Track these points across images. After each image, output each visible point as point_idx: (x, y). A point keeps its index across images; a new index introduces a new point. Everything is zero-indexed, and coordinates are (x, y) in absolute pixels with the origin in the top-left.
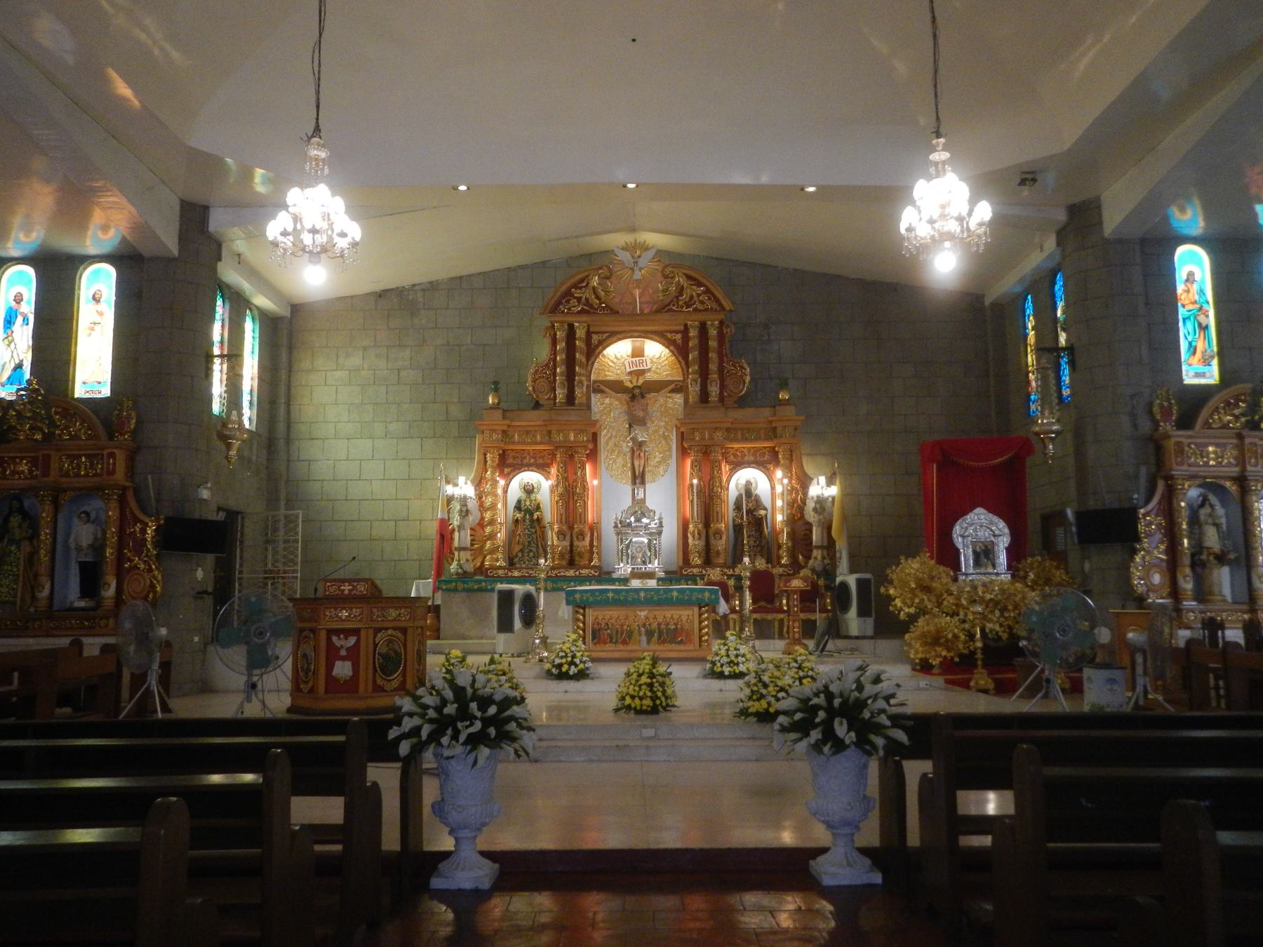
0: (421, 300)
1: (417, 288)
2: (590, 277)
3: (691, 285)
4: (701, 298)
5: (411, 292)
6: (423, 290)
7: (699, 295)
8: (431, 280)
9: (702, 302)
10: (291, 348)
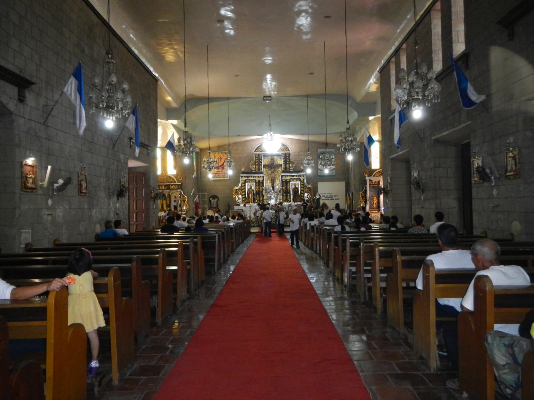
9: (285, 149)
10: (200, 158)
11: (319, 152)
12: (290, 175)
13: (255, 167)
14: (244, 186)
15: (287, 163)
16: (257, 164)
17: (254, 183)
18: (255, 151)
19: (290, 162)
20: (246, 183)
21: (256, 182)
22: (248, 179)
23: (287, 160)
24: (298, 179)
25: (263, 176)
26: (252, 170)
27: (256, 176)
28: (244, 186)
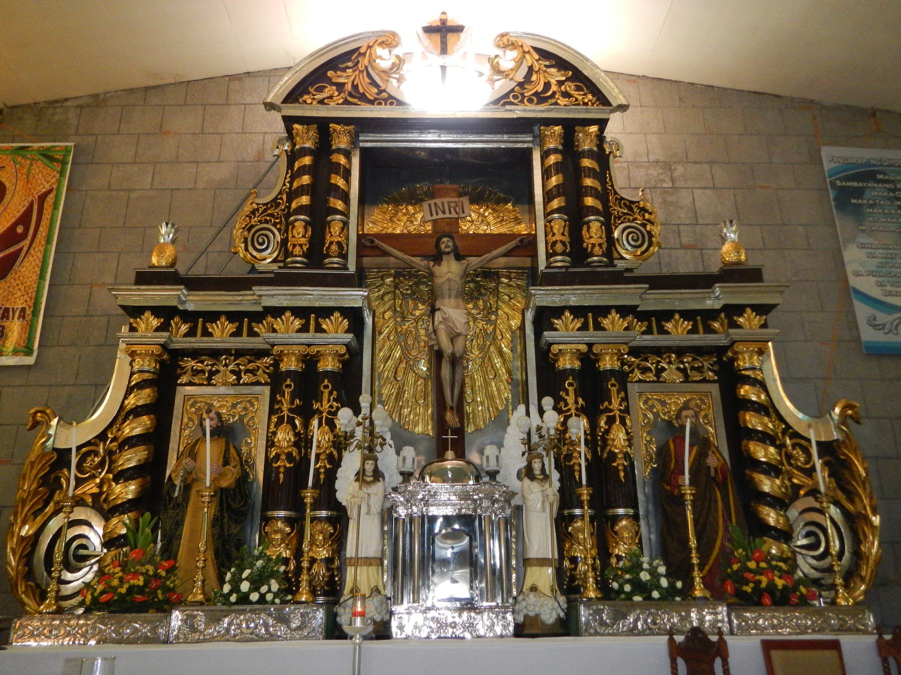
0: (73, 121)
1: (69, 104)
2: (362, 51)
3: (546, 66)
4: (563, 88)
5: (57, 110)
6: (81, 107)
7: (560, 83)
8: (95, 92)
9: (566, 95)
11: (827, 166)
12: (624, 311)
13: (284, 242)
14: (137, 412)
15: (593, 211)
16: (301, 210)
17: (267, 390)
18: (293, 96)
19: (616, 210)
20: (183, 392)
21: (276, 380)
22: (198, 342)
24: (698, 351)
25: (354, 317)
26: (253, 269)
27: (277, 312)
28: (137, 412)
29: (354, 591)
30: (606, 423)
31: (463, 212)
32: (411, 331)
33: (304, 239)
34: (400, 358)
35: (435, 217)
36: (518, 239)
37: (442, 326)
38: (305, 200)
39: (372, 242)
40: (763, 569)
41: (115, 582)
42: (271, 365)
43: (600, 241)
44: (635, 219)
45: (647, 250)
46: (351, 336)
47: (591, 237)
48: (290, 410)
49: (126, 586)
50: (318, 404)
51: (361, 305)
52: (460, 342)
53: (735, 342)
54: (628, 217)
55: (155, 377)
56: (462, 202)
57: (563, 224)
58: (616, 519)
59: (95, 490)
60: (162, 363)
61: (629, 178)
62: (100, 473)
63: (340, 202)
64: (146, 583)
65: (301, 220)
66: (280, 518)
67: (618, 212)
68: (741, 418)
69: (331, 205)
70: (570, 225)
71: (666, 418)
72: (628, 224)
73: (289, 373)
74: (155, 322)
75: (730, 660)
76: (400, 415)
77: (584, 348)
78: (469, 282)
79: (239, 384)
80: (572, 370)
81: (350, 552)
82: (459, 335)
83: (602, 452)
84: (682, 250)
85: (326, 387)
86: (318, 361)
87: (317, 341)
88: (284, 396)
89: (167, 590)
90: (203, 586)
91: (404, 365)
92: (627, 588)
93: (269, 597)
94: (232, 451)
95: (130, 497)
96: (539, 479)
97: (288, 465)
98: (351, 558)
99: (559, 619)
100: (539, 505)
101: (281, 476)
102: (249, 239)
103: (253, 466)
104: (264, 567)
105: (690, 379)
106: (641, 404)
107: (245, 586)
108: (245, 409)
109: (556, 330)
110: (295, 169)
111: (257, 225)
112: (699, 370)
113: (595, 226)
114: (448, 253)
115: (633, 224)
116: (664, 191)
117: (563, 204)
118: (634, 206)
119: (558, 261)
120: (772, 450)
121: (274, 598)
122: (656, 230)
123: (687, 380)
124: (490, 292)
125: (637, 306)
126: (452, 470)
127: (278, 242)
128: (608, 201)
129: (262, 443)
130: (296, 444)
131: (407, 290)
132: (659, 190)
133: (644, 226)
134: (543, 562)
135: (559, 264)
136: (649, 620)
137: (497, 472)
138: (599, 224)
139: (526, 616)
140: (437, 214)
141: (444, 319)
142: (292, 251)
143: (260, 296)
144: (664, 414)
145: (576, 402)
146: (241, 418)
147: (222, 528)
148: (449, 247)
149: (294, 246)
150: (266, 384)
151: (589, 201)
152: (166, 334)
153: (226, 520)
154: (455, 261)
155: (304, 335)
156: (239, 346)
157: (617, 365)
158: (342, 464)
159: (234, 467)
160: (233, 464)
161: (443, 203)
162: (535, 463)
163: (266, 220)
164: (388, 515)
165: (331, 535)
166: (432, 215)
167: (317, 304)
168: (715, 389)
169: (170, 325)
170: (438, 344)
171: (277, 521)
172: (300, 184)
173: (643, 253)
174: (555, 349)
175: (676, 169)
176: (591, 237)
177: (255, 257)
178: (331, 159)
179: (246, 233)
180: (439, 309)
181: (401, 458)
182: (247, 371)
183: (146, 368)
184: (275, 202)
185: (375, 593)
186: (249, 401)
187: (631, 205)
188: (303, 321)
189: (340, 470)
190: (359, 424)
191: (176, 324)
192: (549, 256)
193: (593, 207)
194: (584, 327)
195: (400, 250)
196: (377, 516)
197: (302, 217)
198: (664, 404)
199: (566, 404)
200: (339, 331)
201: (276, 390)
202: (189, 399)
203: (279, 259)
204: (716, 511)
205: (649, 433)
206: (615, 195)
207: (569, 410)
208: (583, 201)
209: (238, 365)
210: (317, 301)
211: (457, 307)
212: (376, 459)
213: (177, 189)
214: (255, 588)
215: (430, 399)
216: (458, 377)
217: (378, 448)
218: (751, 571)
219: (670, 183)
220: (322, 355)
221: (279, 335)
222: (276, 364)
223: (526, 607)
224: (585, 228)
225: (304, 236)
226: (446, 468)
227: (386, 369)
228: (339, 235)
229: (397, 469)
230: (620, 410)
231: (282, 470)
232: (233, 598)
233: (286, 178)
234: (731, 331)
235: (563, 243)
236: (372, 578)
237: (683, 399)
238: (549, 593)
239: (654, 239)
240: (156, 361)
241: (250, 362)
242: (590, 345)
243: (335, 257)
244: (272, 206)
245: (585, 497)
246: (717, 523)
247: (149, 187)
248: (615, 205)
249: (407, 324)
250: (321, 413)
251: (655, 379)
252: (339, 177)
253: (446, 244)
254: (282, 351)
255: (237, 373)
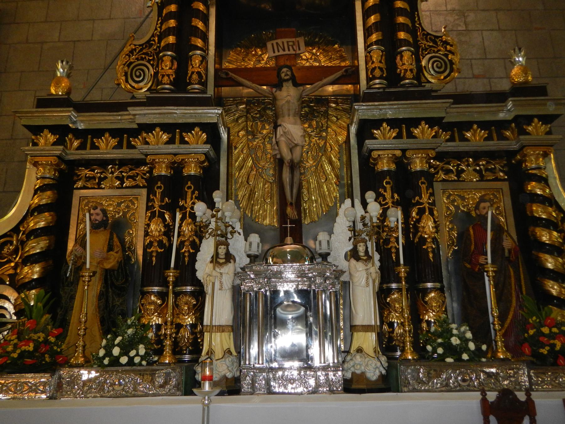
12: (432, 122)
13: (156, 74)
15: (405, 42)
16: (168, 47)
17: (144, 192)
19: (423, 43)
22: (89, 154)
23: (401, 20)
24: (491, 155)
26: (133, 97)
27: (149, 128)
29: (210, 353)
30: (417, 214)
31: (299, 49)
32: (259, 146)
33: (171, 71)
34: (251, 167)
35: (277, 54)
36: (344, 70)
37: (283, 139)
38: (171, 39)
39: (227, 74)
40: (555, 333)
41: (10, 348)
42: (147, 172)
43: (411, 67)
44: (439, 50)
45: (449, 75)
46: (209, 146)
47: (404, 64)
48: (161, 207)
49: (18, 351)
50: (184, 202)
51: (216, 121)
52: (297, 151)
53: (525, 146)
54: (433, 49)
55: (54, 182)
56: (298, 41)
57: (381, 54)
58: (426, 291)
59: (11, 272)
60: (61, 171)
61: (431, 23)
62: (15, 258)
63: (200, 40)
64: (36, 349)
65: (168, 55)
66: (153, 293)
67: (425, 45)
68: (528, 209)
69: (193, 43)
70: (385, 55)
71: (465, 210)
72: (434, 54)
73: (160, 177)
74: (52, 138)
75: (537, 418)
76: (252, 211)
77: (398, 153)
78: (305, 107)
79: (122, 188)
80: (389, 172)
81: (206, 321)
82: (296, 145)
83: (414, 237)
84: (474, 80)
85: (189, 188)
86: (184, 167)
87: (181, 151)
88: (156, 196)
89: (54, 354)
90: (84, 351)
91: (255, 173)
92: (440, 351)
93: (137, 360)
94: (115, 239)
95: (35, 277)
96: (363, 259)
97: (159, 250)
98: (207, 326)
99: (382, 376)
100: (364, 282)
101: (154, 259)
102: (129, 73)
103: (134, 252)
104: (134, 335)
105: (485, 179)
106: (444, 199)
107: (116, 351)
108: (128, 207)
109: (376, 138)
110: (164, 15)
111: (135, 62)
112: (492, 171)
113: (407, 56)
114: (287, 80)
115: (437, 55)
116: (460, 33)
117: (380, 38)
118: (438, 40)
119: (376, 84)
120: (555, 233)
121: (142, 360)
122: (456, 59)
123: (482, 178)
124: (322, 115)
125: (443, 118)
126: (291, 253)
127: (151, 75)
128: (417, 36)
129: (141, 233)
130: (165, 234)
131: (256, 114)
132: (455, 32)
133: (446, 56)
134: (367, 328)
135: (377, 86)
136: (459, 378)
137: (328, 254)
138: (410, 54)
139: (353, 373)
140: (279, 51)
141: (284, 132)
142: (162, 80)
143: (135, 115)
144: (464, 207)
145: (393, 197)
146: (125, 214)
147: (107, 301)
148: (288, 75)
149: (163, 76)
150: (144, 187)
151: (402, 35)
152: (61, 147)
153: (110, 294)
154: (293, 87)
155: (171, 146)
156: (120, 156)
157: (426, 167)
158: (201, 249)
159: (117, 252)
160: (115, 251)
161: (283, 43)
162: (360, 246)
163: (142, 57)
164: (236, 291)
165: (195, 305)
166: (274, 52)
167: (180, 121)
168: (505, 186)
169: (65, 141)
170: (280, 153)
171: (151, 295)
172: (167, 27)
173: (445, 78)
174: (375, 154)
175: (468, 16)
176: (404, 64)
177: (133, 87)
178: (192, 7)
179: (126, 68)
180: (280, 125)
181: (248, 243)
182: (128, 177)
183: (48, 175)
184: (148, 44)
185: (227, 355)
186: (131, 201)
187: (435, 39)
188: (170, 135)
189: (199, 253)
190: (213, 216)
191: (70, 140)
192: (369, 80)
193: (405, 40)
194: (399, 136)
195: (249, 80)
196: (228, 291)
197: (169, 53)
198: (463, 198)
199: (385, 199)
200: (199, 143)
201: (151, 192)
202: (83, 200)
203: (153, 88)
204: (510, 284)
205: (451, 222)
206: (422, 32)
207: (387, 204)
208: (396, 35)
209: (121, 172)
210: (180, 118)
211: (295, 123)
212: (227, 245)
213: (79, 41)
214: (125, 353)
215: (275, 199)
216: (296, 179)
217: (229, 236)
218: (544, 335)
219: (464, 26)
220: (186, 162)
221: (151, 147)
222: (151, 171)
223: (353, 366)
224: (398, 58)
225: (170, 68)
226: (286, 251)
227: (240, 176)
228: (199, 67)
229: (245, 252)
230: (429, 203)
231: (154, 254)
232: (106, 361)
233: (157, 24)
234: (522, 137)
235: (381, 69)
236: (224, 342)
237: (478, 195)
238: (373, 355)
239: (454, 66)
240: (55, 170)
241: (131, 170)
242: (404, 151)
243: (196, 84)
244: (146, 47)
245: (403, 275)
246: (511, 294)
247: (57, 40)
248: (423, 39)
249: (257, 140)
250: (186, 208)
251: (456, 178)
252: (198, 20)
253: (285, 73)
254: (153, 160)
255: (121, 179)
